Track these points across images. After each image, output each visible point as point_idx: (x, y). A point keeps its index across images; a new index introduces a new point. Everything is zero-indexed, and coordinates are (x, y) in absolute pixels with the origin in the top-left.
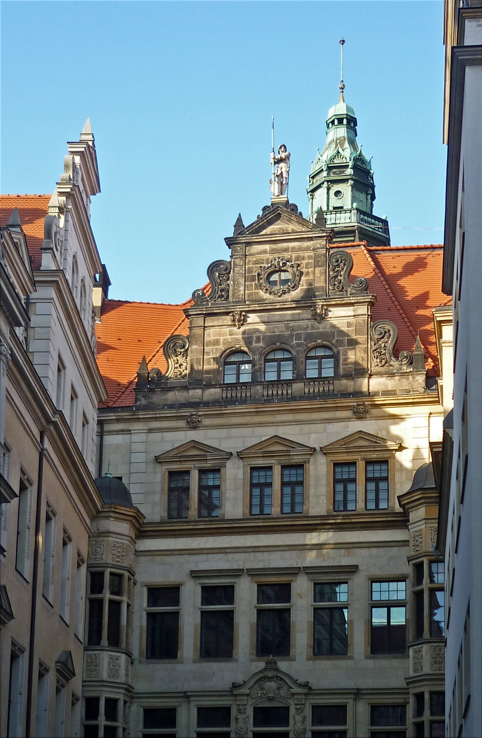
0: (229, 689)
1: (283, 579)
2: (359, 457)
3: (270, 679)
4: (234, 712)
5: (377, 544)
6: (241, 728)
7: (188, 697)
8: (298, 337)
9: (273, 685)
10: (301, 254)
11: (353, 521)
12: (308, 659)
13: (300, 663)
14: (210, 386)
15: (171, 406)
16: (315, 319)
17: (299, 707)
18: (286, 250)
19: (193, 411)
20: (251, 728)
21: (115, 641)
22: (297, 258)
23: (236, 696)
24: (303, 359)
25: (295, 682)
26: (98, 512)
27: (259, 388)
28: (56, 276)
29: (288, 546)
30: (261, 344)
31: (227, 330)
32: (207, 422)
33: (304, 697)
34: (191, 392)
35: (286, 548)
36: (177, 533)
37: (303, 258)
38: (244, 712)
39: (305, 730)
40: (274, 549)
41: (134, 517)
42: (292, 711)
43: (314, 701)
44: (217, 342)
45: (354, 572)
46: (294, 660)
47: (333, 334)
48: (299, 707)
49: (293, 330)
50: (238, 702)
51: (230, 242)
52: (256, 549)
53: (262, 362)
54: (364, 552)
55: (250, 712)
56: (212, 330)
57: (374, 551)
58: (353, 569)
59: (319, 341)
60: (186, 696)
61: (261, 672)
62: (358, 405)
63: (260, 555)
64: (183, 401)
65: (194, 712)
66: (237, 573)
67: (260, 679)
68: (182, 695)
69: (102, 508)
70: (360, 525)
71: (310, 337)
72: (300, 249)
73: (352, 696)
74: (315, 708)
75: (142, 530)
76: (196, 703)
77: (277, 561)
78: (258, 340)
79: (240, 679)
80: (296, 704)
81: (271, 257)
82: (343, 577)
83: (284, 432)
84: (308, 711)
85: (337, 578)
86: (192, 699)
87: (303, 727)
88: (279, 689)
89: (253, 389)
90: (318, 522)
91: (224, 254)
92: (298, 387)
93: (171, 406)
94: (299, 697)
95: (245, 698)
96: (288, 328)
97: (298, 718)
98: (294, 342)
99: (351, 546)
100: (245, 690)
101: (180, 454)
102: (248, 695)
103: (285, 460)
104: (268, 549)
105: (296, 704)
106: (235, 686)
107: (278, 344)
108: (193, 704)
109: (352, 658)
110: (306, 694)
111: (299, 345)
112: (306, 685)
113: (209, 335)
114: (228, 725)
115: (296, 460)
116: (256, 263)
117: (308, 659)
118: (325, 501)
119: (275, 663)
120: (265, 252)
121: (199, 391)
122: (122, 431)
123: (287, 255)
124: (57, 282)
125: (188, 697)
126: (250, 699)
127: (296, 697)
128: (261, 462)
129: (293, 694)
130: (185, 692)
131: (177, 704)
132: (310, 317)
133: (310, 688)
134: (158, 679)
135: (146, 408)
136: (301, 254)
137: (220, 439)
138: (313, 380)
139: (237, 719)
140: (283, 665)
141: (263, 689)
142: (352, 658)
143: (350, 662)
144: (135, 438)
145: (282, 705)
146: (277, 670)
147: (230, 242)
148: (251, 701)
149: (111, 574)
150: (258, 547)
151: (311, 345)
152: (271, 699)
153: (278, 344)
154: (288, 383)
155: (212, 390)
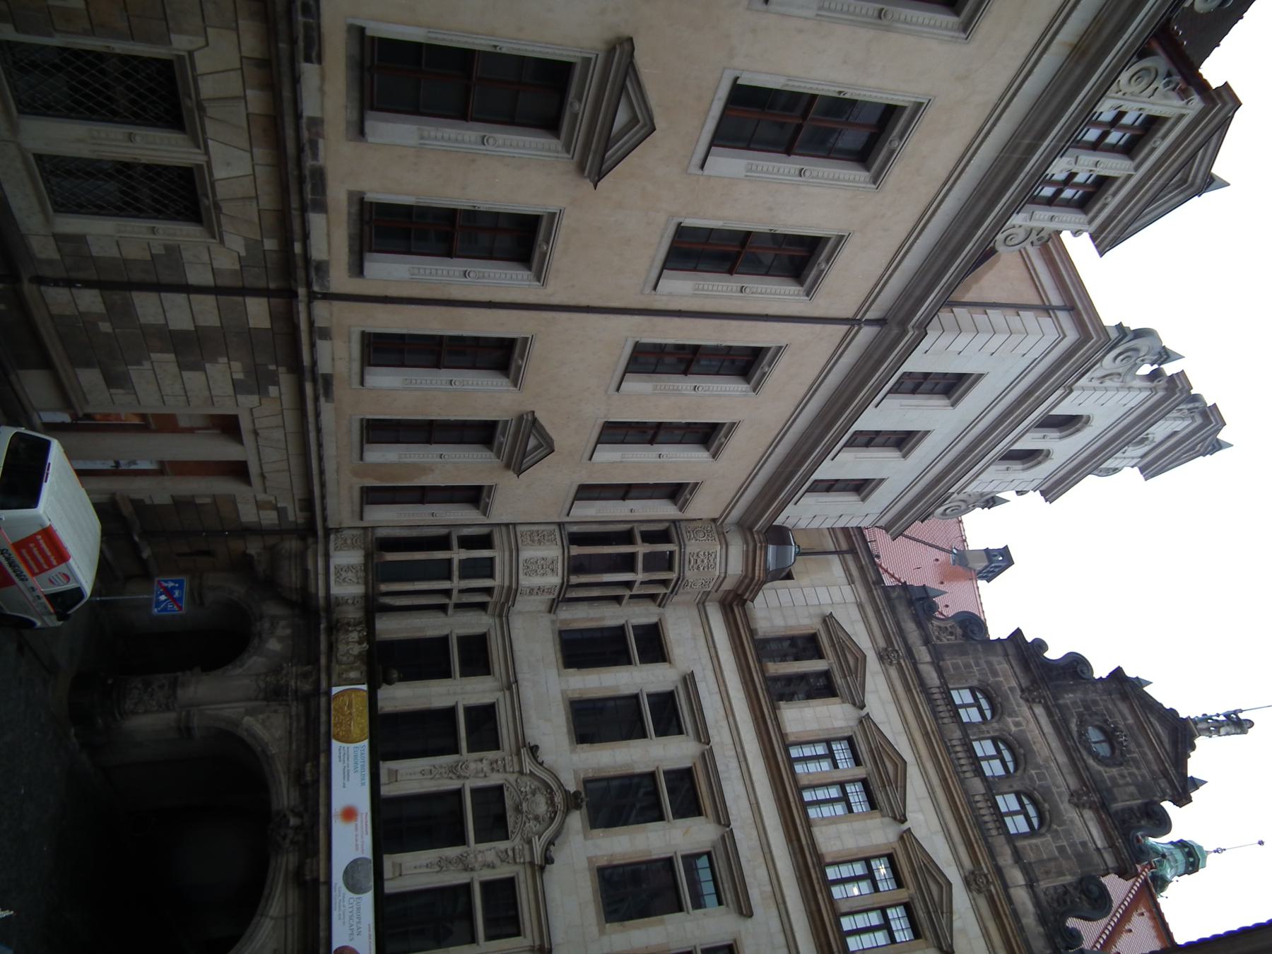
0: (528, 740)
1: (706, 802)
2: (912, 891)
3: (551, 802)
4: (491, 755)
5: (791, 944)
6: (467, 768)
7: (509, 688)
8: (1041, 776)
9: (542, 808)
10: (1143, 765)
11: (819, 896)
12: (590, 859)
13: (585, 849)
14: (940, 671)
15: (898, 624)
16: (1072, 795)
17: (510, 853)
18: (1139, 745)
19: (902, 652)
20: (469, 785)
21: (576, 566)
22: (1134, 760)
23: (518, 753)
24: (1016, 788)
25: (551, 843)
26: (750, 529)
27: (957, 734)
28: (1098, 335)
29: (757, 803)
30: (1013, 729)
31: (1014, 684)
32: (894, 672)
33: (528, 859)
34: (923, 649)
35: (753, 801)
36: (740, 650)
37: (1138, 768)
38: (493, 770)
39: (472, 870)
40: (748, 783)
41: (753, 578)
42: (502, 845)
43: (522, 878)
44: (995, 674)
45: (741, 913)
46: (585, 838)
47: (1062, 823)
48: (510, 853)
49: (1047, 768)
50: (508, 759)
51: (1118, 674)
52: (742, 758)
53: (992, 734)
54: (775, 925)
55: (495, 779)
56: (1006, 666)
57: (780, 939)
58: (745, 910)
59: (1046, 806)
60: (511, 685)
61: (561, 785)
62: (986, 876)
63: (734, 764)
64: (910, 641)
65: (487, 700)
66: (702, 735)
67: (548, 786)
68: (512, 679)
69: (758, 532)
70: (814, 908)
71: (1047, 792)
72: (1148, 763)
73: (537, 943)
74: (510, 883)
75: (735, 602)
76: (501, 699)
77: (733, 790)
78: (1017, 724)
79: (546, 756)
80: (513, 850)
81: (1121, 726)
82: (728, 895)
83: (913, 772)
84: (503, 872)
85: (726, 886)
86: (507, 693)
87: (477, 865)
88: (536, 818)
89: (954, 727)
90: (804, 842)
91: (1101, 670)
92: (977, 785)
93: (898, 624)
94: (527, 852)
95: (517, 768)
96: (1046, 761)
97: (490, 857)
98: (1033, 772)
99: (780, 901)
100: (528, 766)
101: (844, 645)
102: (521, 772)
103: (875, 784)
104: (746, 775)
105: (513, 850)
106: (534, 750)
107: (1022, 751)
108: (499, 695)
109: (602, 932)
110: (532, 863)
111: (1031, 779)
112: (548, 860)
113: (1000, 663)
114: (471, 749)
115: (880, 797)
116: (1107, 709)
117: (590, 859)
118: (835, 849)
119: (578, 807)
120: (1125, 719)
121: (928, 659)
122: (851, 575)
123: (1133, 747)
124: (1089, 337)
125: (509, 688)
126: (515, 776)
127: (526, 847)
128: (863, 748)
129: (529, 842)
130: (516, 681)
131: (497, 673)
132: (1072, 788)
133: (542, 869)
134: (532, 641)
135: (888, 599)
136: (1143, 765)
137: (877, 691)
138: (995, 806)
139: (481, 760)
140: (576, 820)
141: (534, 794)
142: (602, 932)
143: (594, 930)
144: (847, 589)
145: (510, 829)
146: (567, 812)
147: (1118, 674)
148: (512, 778)
149: (672, 553)
150: (746, 760)
151: (1037, 795)
152: (518, 810)
153: (1022, 751)
154: (979, 772)
155: (934, 675)
